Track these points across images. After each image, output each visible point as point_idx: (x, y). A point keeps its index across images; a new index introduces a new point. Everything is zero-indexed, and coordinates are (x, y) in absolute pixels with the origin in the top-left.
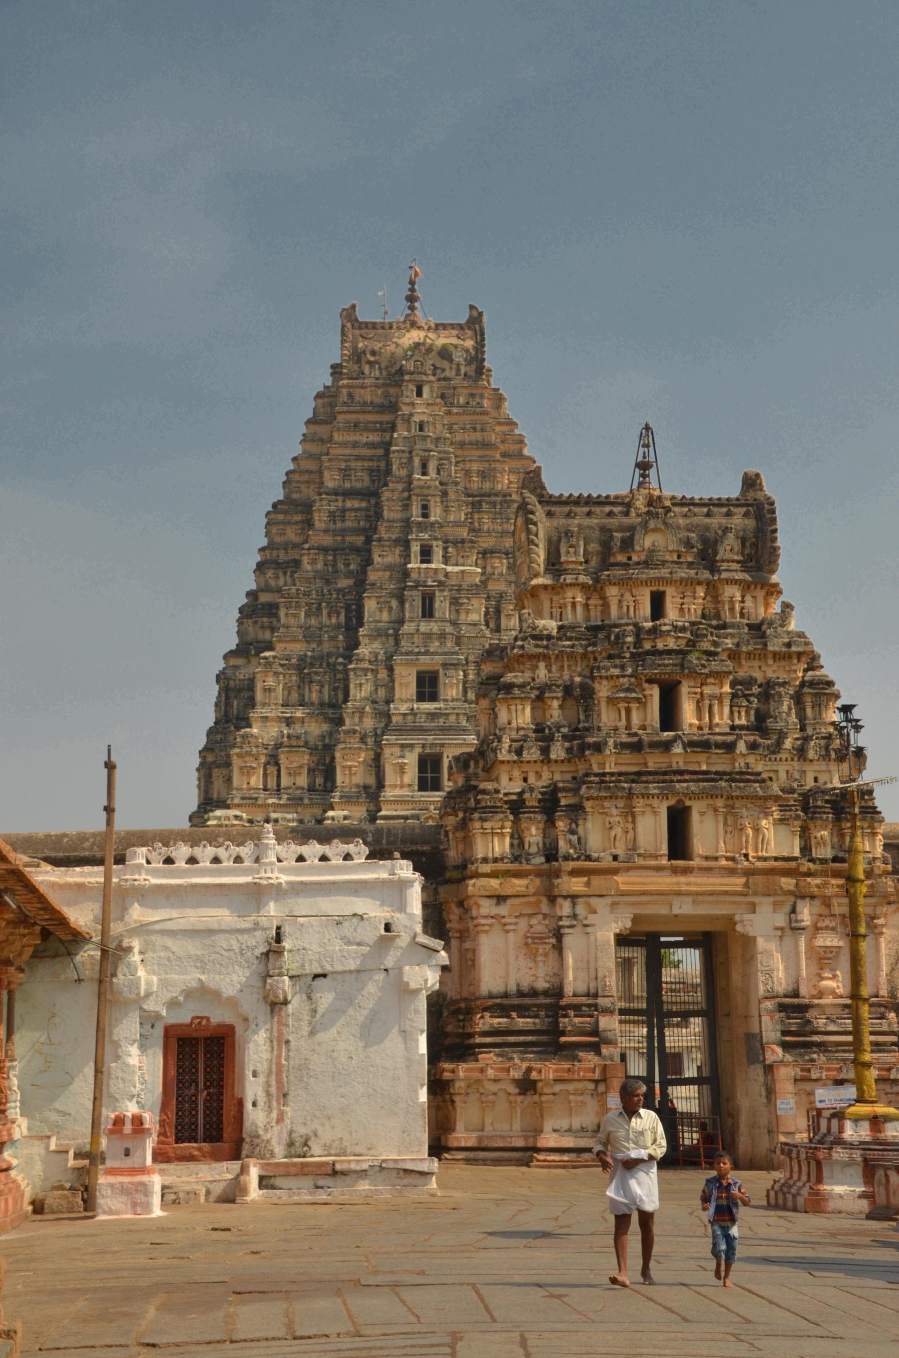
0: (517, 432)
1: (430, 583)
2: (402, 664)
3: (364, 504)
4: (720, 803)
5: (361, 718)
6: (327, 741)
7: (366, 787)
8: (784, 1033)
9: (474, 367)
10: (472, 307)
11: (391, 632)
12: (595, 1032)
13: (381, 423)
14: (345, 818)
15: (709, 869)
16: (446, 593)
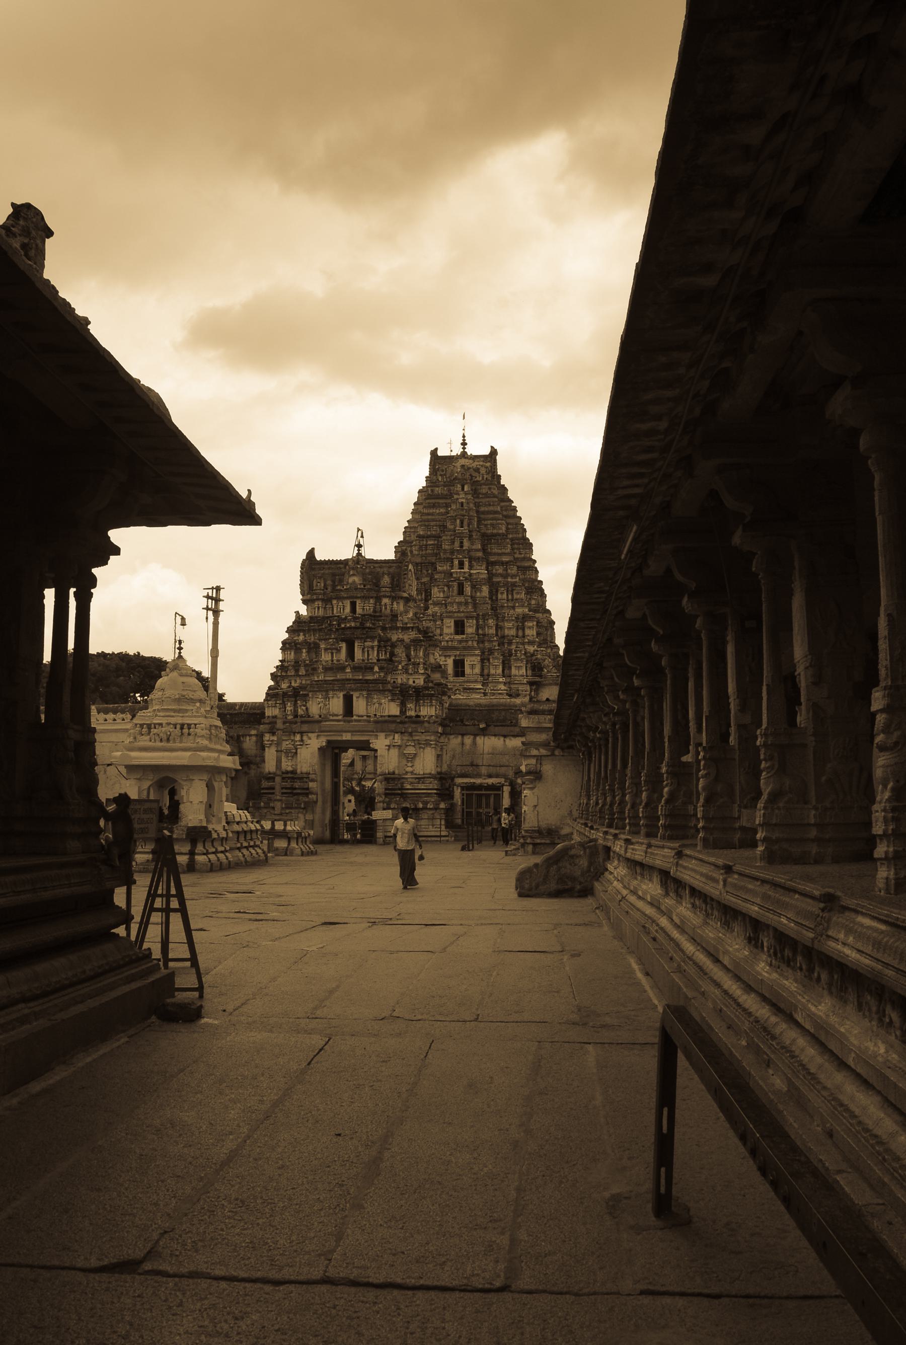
4: (365, 693)
8: (386, 789)
10: (492, 447)
12: (308, 789)
15: (359, 721)
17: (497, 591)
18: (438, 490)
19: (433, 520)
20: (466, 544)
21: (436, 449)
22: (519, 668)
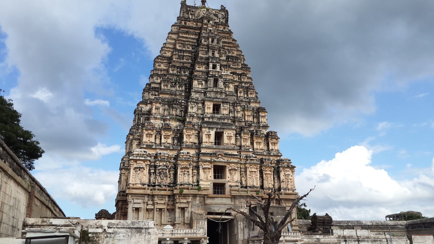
0: (237, 43)
1: (217, 76)
2: (208, 101)
3: (190, 55)
7: (194, 143)
14: (188, 153)
16: (222, 80)
18: (189, 24)
19: (187, 41)
20: (217, 55)
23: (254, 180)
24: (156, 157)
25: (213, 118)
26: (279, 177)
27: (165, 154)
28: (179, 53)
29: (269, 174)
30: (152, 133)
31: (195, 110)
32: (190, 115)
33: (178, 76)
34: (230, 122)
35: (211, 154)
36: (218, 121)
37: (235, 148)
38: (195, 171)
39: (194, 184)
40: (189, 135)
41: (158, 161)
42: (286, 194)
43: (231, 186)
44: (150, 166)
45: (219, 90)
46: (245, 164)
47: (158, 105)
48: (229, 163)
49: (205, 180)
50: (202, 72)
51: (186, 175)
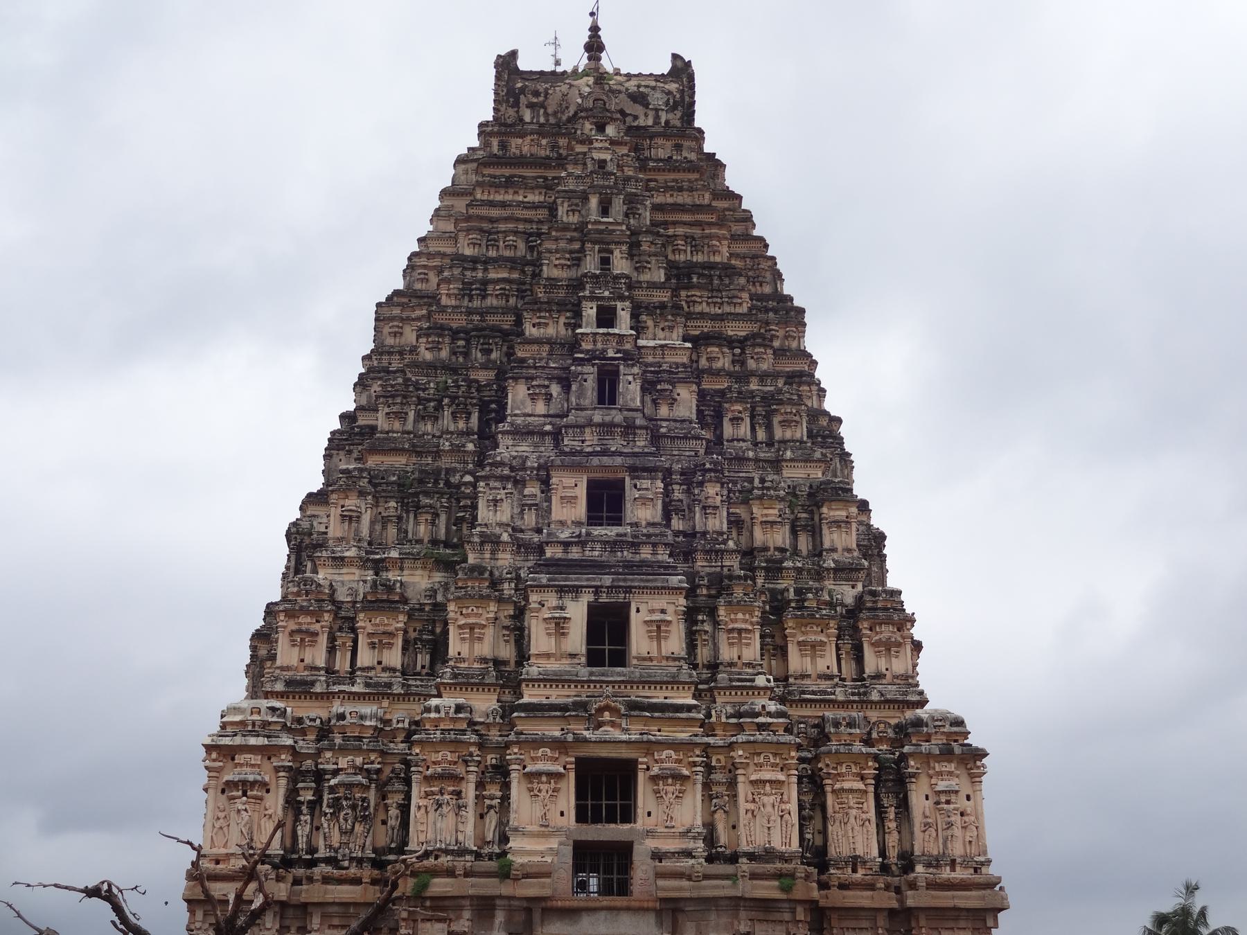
1: (611, 354)
2: (563, 467)
3: (515, 276)
5: (493, 552)
6: (440, 598)
7: (497, 663)
9: (679, 114)
10: (675, 57)
11: (548, 428)
13: (546, 178)
14: (459, 708)
16: (636, 370)
17: (719, 416)
20: (620, 265)
21: (513, 54)
22: (814, 648)
23: (768, 820)
24: (324, 732)
25: (582, 543)
26: (904, 805)
27: (362, 717)
28: (468, 273)
29: (851, 791)
30: (317, 627)
31: (505, 513)
32: (482, 535)
33: (453, 370)
34: (663, 556)
35: (563, 708)
36: (606, 557)
37: (684, 677)
38: (494, 790)
39: (486, 850)
40: (472, 627)
41: (331, 748)
42: (933, 885)
43: (658, 856)
44: (295, 775)
45: (619, 418)
46: (731, 746)
47: (352, 502)
48: (650, 747)
49: (535, 828)
50: (549, 341)
51: (445, 809)
